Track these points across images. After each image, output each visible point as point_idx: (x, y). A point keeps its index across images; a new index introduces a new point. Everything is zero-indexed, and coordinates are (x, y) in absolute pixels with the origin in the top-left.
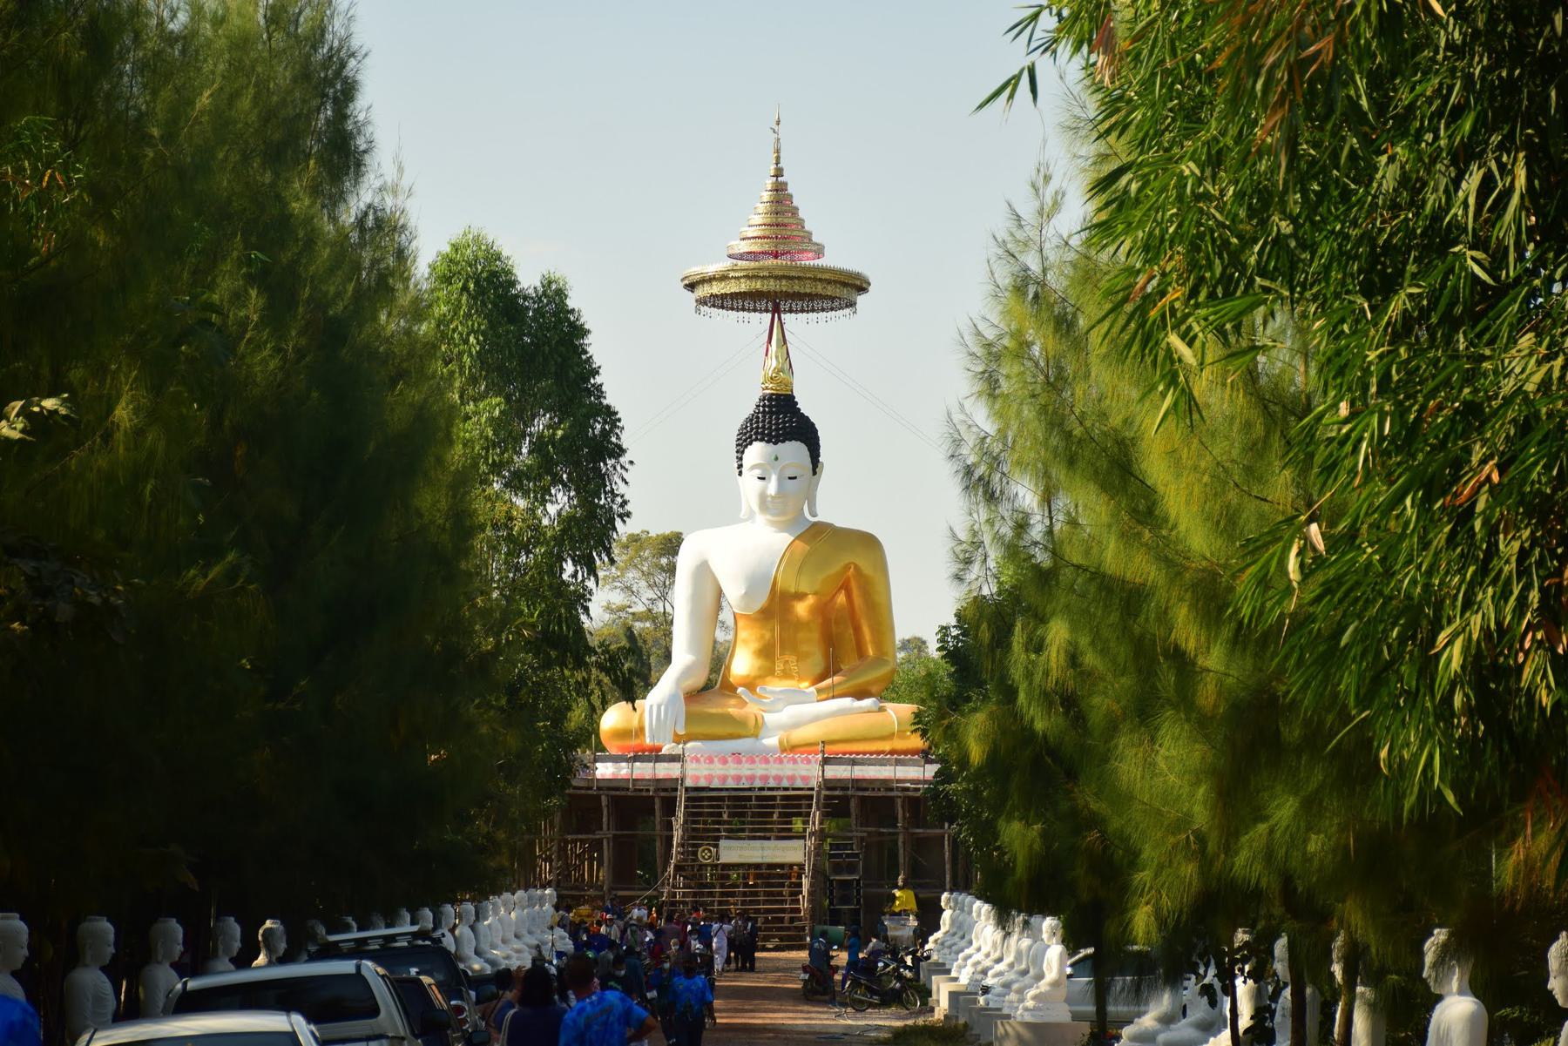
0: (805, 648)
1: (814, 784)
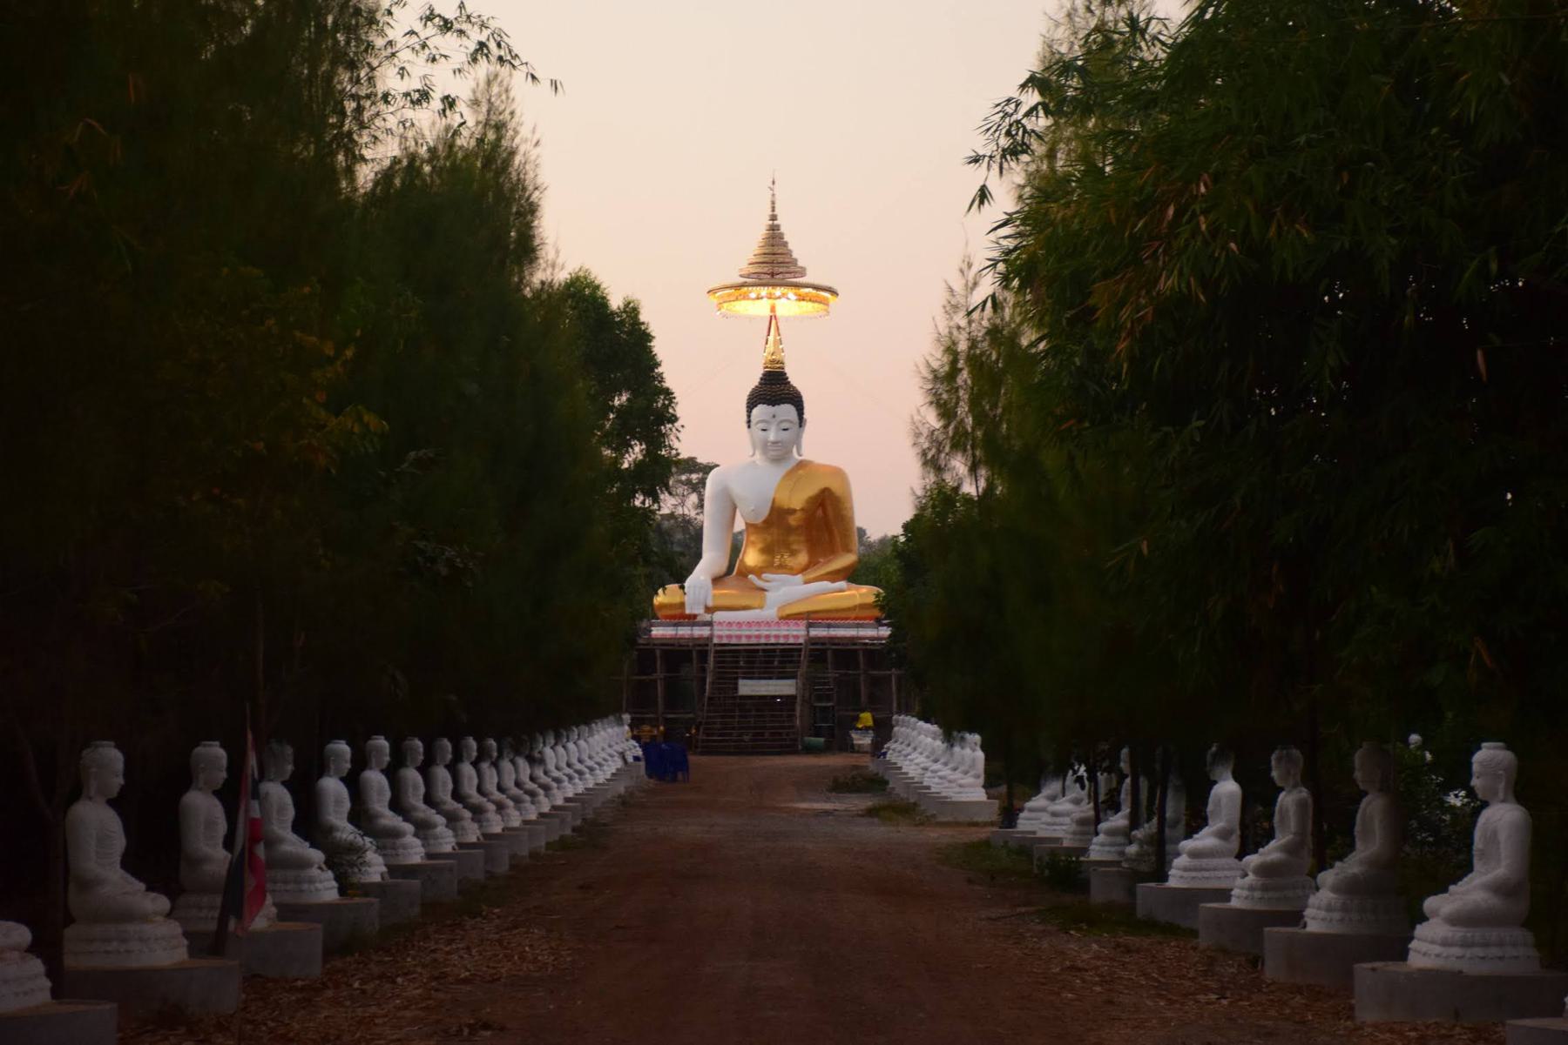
0: (795, 547)
1: (801, 641)
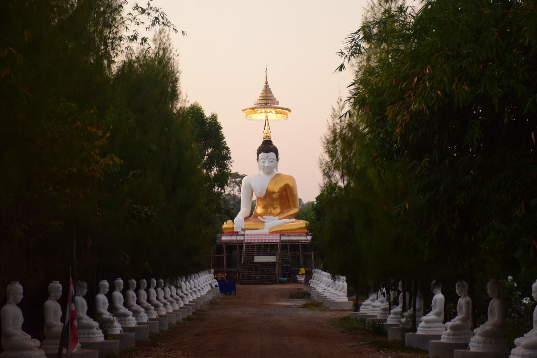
0: (275, 206)
1: (278, 241)
